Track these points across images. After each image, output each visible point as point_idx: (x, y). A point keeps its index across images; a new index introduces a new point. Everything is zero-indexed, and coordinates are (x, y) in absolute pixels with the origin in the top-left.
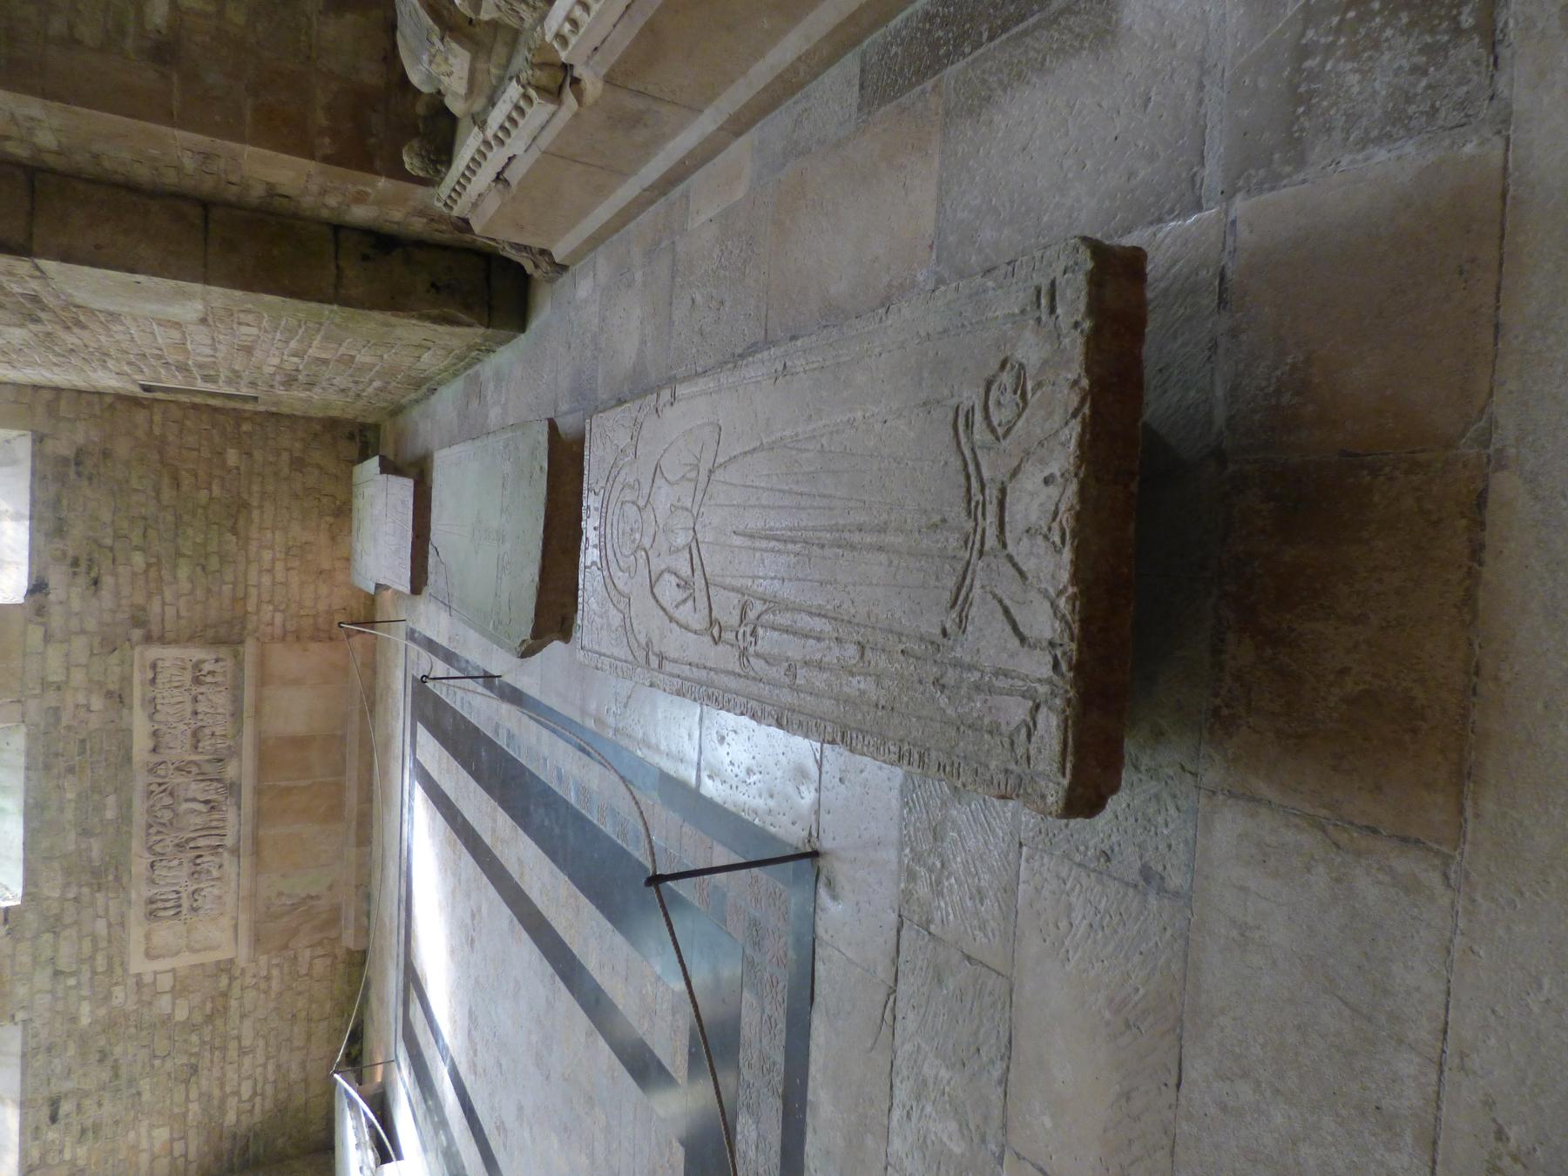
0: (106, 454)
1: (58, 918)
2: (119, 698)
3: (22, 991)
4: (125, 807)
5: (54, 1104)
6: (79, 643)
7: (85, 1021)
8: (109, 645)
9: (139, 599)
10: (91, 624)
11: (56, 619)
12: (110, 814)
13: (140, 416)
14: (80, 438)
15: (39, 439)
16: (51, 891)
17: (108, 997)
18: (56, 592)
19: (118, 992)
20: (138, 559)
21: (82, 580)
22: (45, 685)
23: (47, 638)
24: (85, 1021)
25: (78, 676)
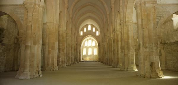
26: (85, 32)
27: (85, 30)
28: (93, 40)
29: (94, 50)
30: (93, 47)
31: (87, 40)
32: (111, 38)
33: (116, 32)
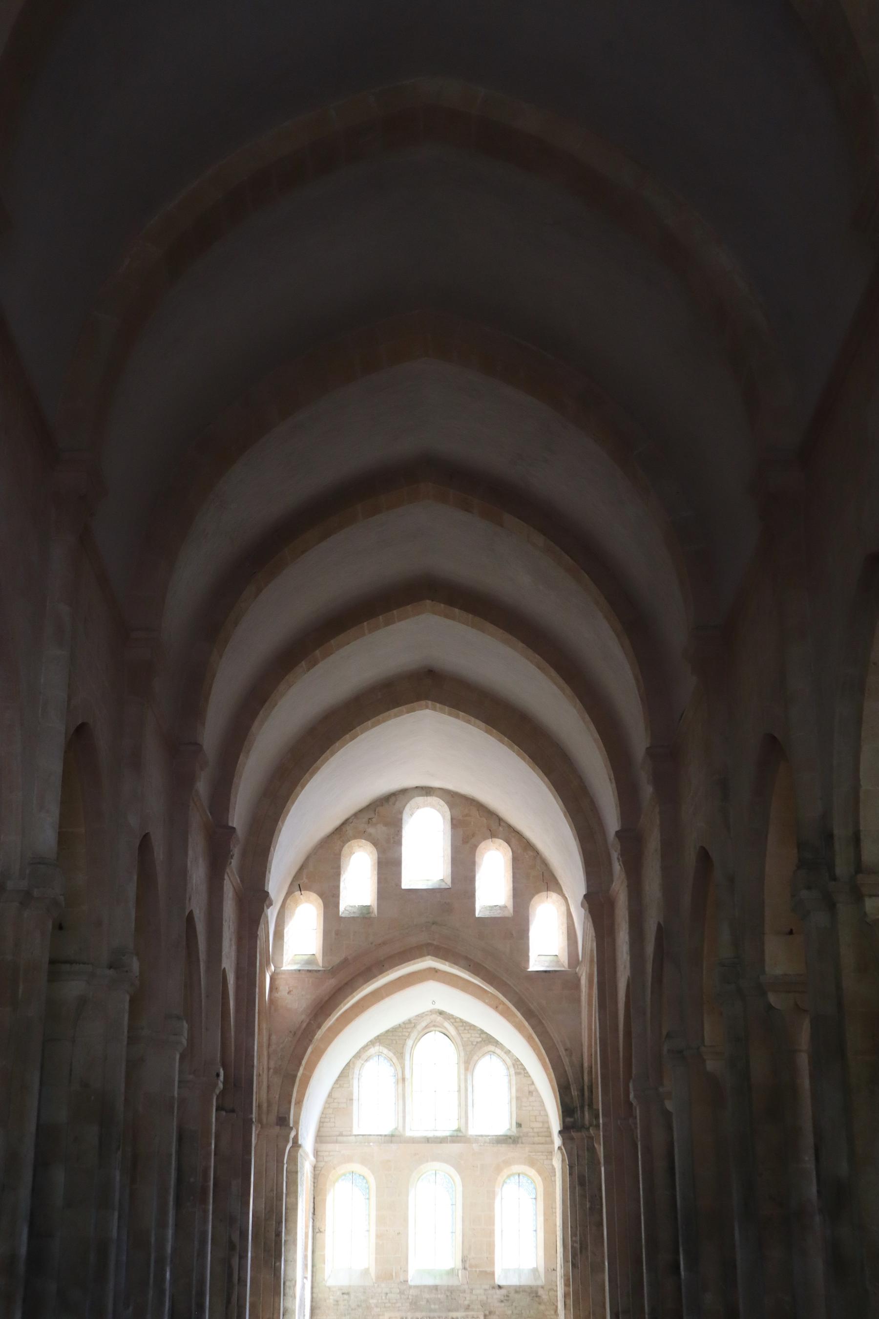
0: (540, 1304)
1: (403, 1294)
2: (468, 1308)
3: (383, 1285)
4: (434, 1311)
5: (348, 1294)
6: (484, 1298)
7: (371, 1301)
8: (483, 1305)
9: (497, 1313)
10: (489, 1301)
11: (491, 1292)
12: (433, 1306)
13: (553, 1312)
14: (544, 1297)
15: (542, 1287)
16: (412, 1292)
17: (377, 1307)
18: (498, 1292)
19: (379, 1309)
20: (509, 1312)
21: (502, 1298)
22: (472, 1290)
23: (485, 1290)
24: (371, 1301)
25: (474, 1297)
26: (364, 916)
27: (358, 882)
28: (489, 1040)
29: (492, 1195)
30: (474, 1158)
31: (395, 1040)
32: (772, 998)
33: (858, 896)
